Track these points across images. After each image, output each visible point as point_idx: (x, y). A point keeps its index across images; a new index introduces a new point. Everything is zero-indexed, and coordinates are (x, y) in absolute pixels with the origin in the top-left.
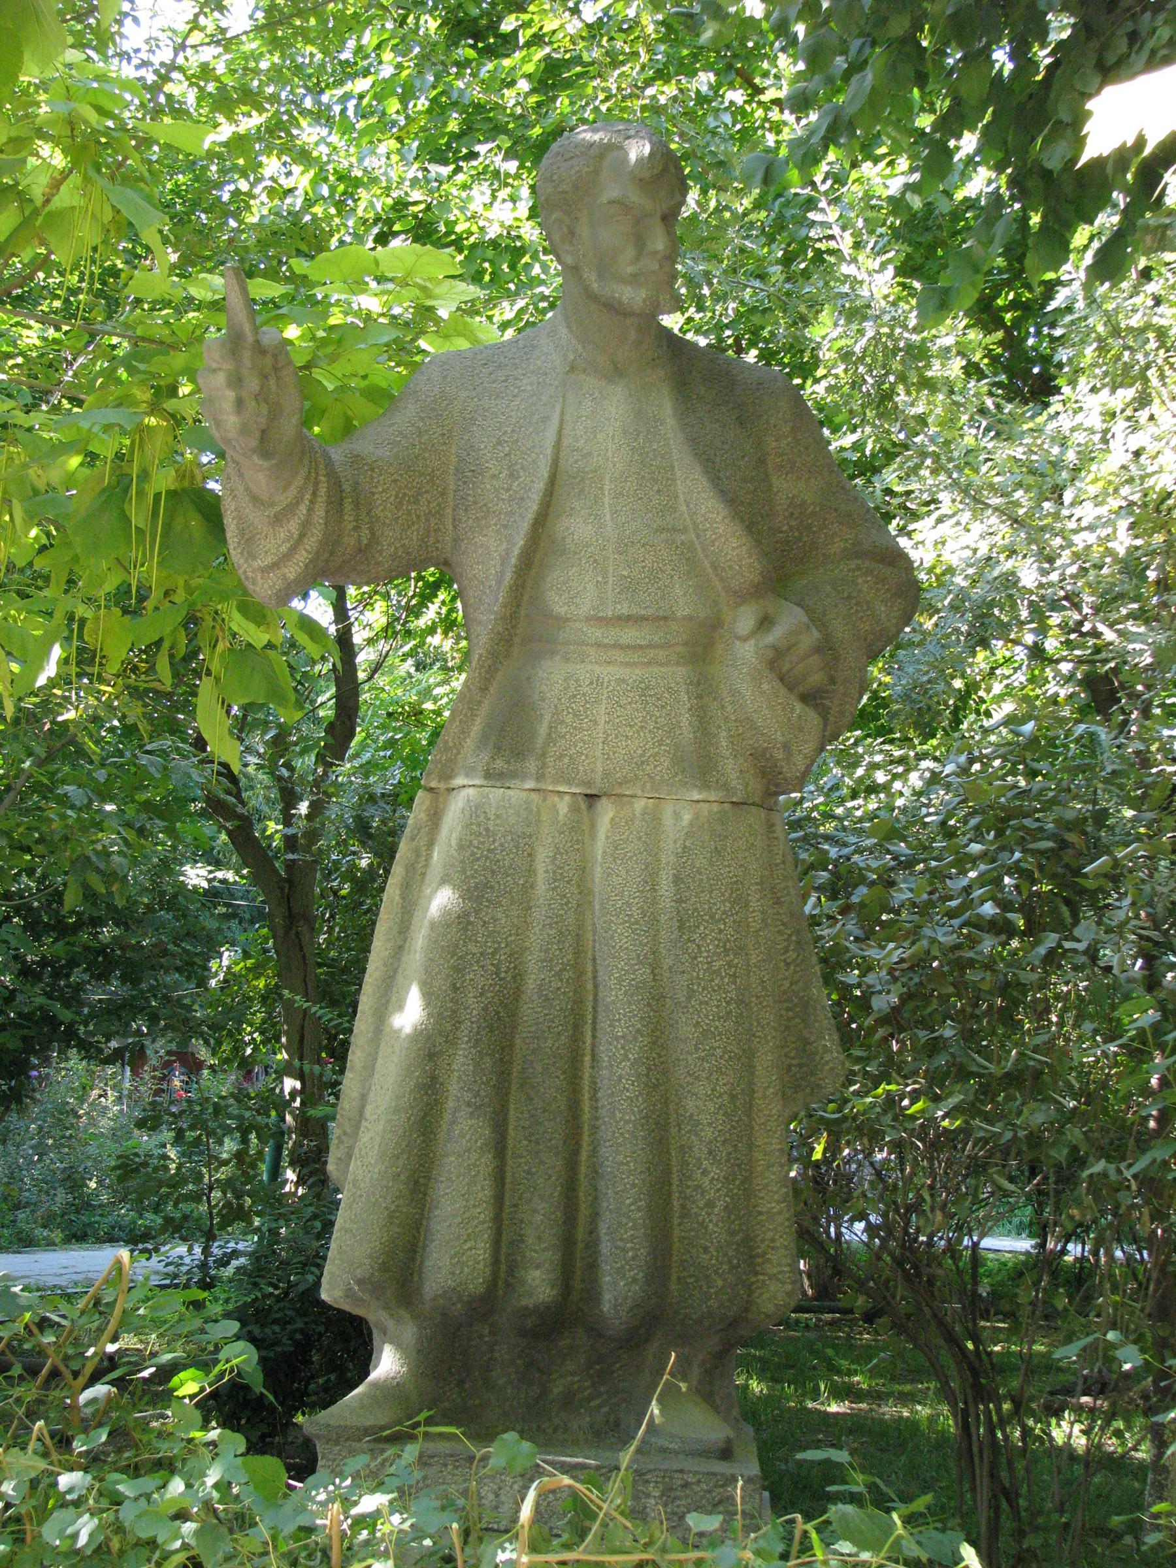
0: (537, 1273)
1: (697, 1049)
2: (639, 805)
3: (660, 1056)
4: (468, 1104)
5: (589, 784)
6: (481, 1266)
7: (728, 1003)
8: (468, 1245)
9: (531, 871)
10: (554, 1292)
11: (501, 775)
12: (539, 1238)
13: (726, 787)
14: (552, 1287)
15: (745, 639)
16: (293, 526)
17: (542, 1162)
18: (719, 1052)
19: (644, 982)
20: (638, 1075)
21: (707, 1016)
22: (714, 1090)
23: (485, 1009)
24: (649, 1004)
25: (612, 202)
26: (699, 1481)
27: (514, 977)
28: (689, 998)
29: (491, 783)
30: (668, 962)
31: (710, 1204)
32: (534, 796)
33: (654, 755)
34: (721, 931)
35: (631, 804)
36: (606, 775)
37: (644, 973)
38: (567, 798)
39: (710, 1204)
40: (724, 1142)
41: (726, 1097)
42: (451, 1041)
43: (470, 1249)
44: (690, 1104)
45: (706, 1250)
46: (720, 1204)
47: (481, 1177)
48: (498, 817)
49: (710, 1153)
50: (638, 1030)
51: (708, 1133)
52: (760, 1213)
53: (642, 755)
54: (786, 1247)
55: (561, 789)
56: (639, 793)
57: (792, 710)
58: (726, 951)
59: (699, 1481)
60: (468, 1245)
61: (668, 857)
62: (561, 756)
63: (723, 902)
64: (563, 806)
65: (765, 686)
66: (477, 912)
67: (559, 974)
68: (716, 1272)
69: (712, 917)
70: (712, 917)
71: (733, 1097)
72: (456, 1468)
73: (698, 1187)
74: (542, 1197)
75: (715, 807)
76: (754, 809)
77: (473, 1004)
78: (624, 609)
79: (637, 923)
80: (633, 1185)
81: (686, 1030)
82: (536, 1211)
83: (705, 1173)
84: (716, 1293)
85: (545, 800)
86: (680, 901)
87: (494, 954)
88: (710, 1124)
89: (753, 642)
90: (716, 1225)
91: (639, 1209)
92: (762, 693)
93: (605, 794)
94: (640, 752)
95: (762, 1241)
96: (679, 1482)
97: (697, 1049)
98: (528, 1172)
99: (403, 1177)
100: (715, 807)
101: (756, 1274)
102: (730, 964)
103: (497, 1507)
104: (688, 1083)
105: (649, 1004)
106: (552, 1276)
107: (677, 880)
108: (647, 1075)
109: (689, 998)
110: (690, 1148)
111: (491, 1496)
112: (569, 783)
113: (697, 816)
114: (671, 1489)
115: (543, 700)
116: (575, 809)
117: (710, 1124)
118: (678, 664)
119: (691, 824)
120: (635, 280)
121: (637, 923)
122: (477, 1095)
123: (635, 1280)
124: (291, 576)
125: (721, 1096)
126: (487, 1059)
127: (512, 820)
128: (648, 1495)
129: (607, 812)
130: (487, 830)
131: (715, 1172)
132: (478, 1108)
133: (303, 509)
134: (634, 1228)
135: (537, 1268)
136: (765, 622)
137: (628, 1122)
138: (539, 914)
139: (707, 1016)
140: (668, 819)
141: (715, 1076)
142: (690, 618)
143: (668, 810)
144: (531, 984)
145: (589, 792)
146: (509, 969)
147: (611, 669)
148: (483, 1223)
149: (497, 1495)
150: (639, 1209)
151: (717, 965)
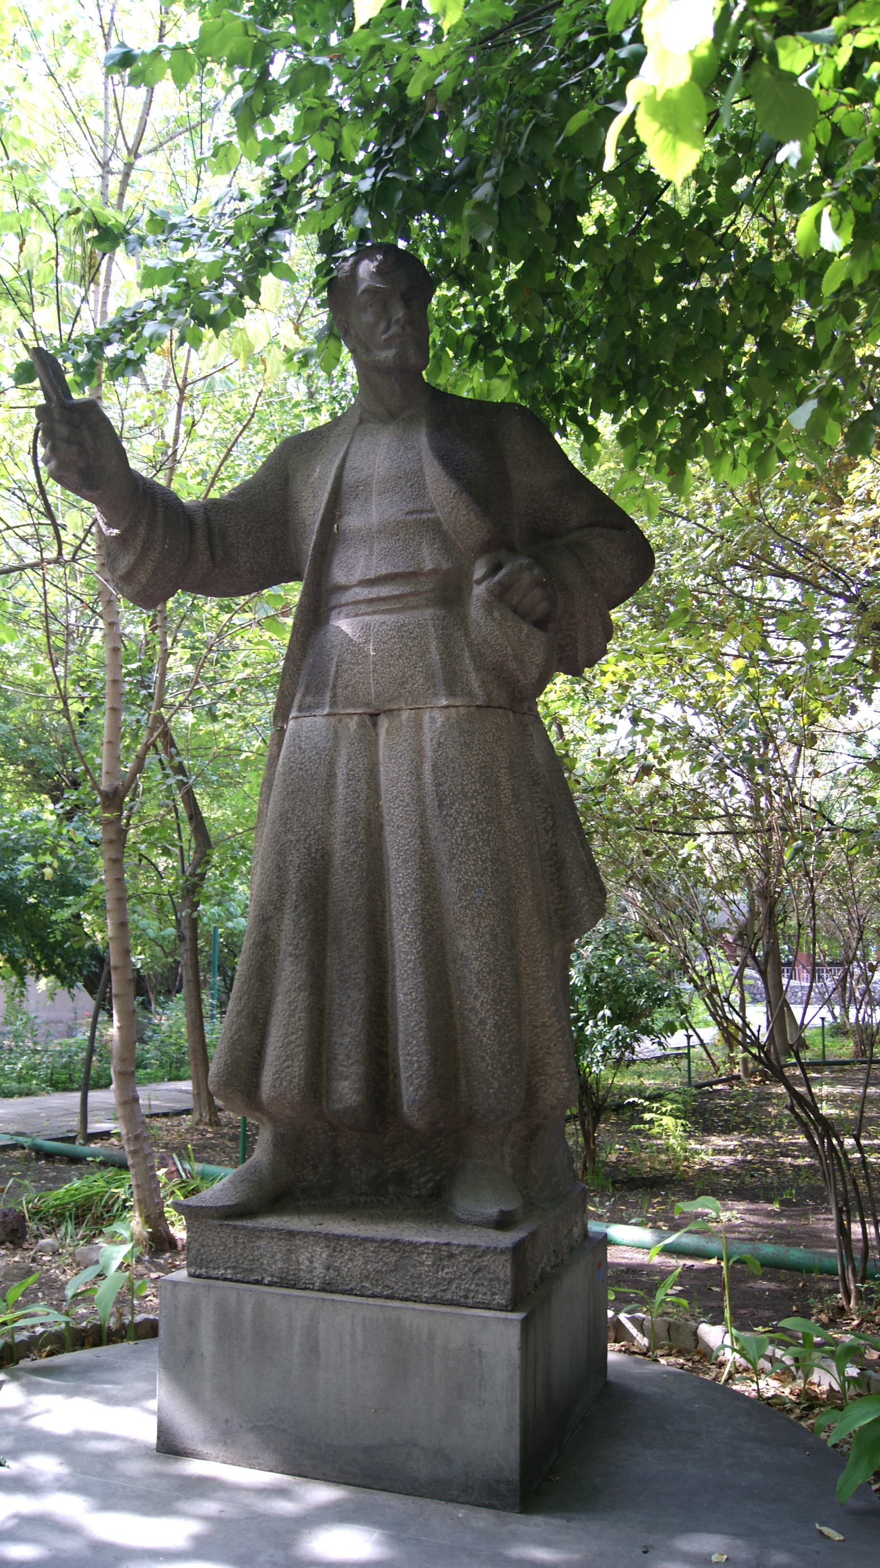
0: (346, 1083)
1: (460, 900)
2: (405, 715)
3: (433, 907)
4: (291, 955)
5: (368, 705)
6: (296, 1081)
7: (483, 862)
8: (287, 1064)
9: (331, 775)
10: (360, 1098)
11: (310, 708)
12: (348, 1057)
13: (470, 694)
14: (358, 1094)
15: (479, 582)
16: (138, 545)
17: (349, 997)
18: (478, 901)
19: (415, 851)
20: (416, 924)
21: (466, 873)
22: (477, 931)
23: (301, 881)
24: (420, 868)
25: (363, 292)
26: (461, 1253)
27: (322, 856)
28: (451, 860)
29: (304, 714)
30: (434, 834)
31: (482, 1022)
32: (332, 720)
33: (411, 676)
34: (473, 806)
35: (399, 716)
36: (378, 696)
37: (415, 843)
38: (355, 718)
39: (482, 1022)
40: (489, 973)
41: (487, 936)
42: (279, 908)
43: (288, 1067)
44: (461, 944)
45: (483, 1059)
46: (490, 1022)
47: (299, 1010)
48: (307, 738)
49: (479, 981)
50: (414, 889)
51: (476, 965)
52: (536, 1027)
53: (403, 677)
54: (560, 1053)
55: (349, 711)
56: (404, 706)
57: (520, 631)
58: (480, 822)
59: (461, 1253)
60: (287, 1064)
61: (429, 753)
62: (346, 687)
63: (474, 783)
64: (353, 724)
65: (496, 614)
66: (293, 810)
67: (354, 851)
68: (492, 1076)
69: (465, 796)
70: (465, 796)
71: (494, 937)
72: (280, 1240)
73: (473, 1009)
74: (350, 1024)
75: (462, 710)
76: (500, 711)
77: (293, 877)
78: (384, 571)
79: (408, 805)
80: (416, 1011)
81: (450, 886)
82: (345, 1035)
83: (476, 997)
84: (494, 1093)
85: (340, 721)
86: (438, 785)
87: (305, 840)
88: (476, 959)
89: (484, 584)
90: (489, 1038)
91: (420, 1030)
92: (494, 620)
93: (385, 712)
94: (400, 674)
95: (541, 1049)
96: (446, 1254)
97: (460, 900)
98: (340, 1005)
99: (244, 1013)
100: (462, 710)
101: (539, 1074)
102: (483, 831)
103: (311, 1272)
104: (457, 928)
105: (420, 868)
106: (357, 1085)
107: (435, 768)
108: (422, 923)
109: (451, 860)
110: (464, 978)
111: (307, 1263)
112: (354, 706)
113: (448, 718)
114: (441, 1259)
115: (333, 647)
116: (361, 725)
117: (476, 959)
118: (427, 606)
119: (443, 725)
120: (387, 344)
121: (408, 805)
122: (296, 947)
123: (420, 1087)
124: (143, 581)
125: (483, 936)
126: (303, 920)
127: (317, 739)
128: (422, 1264)
129: (384, 723)
130: (300, 748)
131: (484, 997)
132: (297, 957)
133: (142, 531)
134: (417, 1045)
135: (346, 1079)
136: (495, 568)
137: (409, 961)
138: (340, 806)
139: (466, 873)
140: (426, 726)
141: (477, 920)
142: (434, 571)
143: (426, 717)
144: (337, 861)
145: (369, 711)
146: (317, 850)
147: (377, 617)
148: (299, 1046)
149: (311, 1262)
150: (420, 1030)
151: (471, 832)
